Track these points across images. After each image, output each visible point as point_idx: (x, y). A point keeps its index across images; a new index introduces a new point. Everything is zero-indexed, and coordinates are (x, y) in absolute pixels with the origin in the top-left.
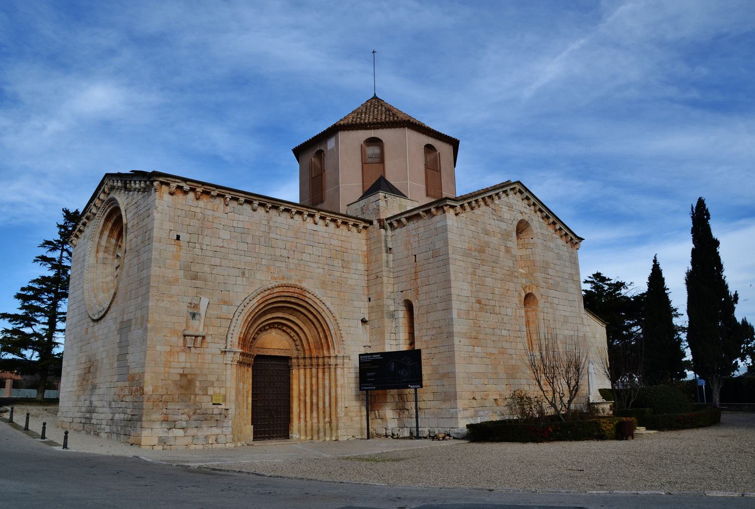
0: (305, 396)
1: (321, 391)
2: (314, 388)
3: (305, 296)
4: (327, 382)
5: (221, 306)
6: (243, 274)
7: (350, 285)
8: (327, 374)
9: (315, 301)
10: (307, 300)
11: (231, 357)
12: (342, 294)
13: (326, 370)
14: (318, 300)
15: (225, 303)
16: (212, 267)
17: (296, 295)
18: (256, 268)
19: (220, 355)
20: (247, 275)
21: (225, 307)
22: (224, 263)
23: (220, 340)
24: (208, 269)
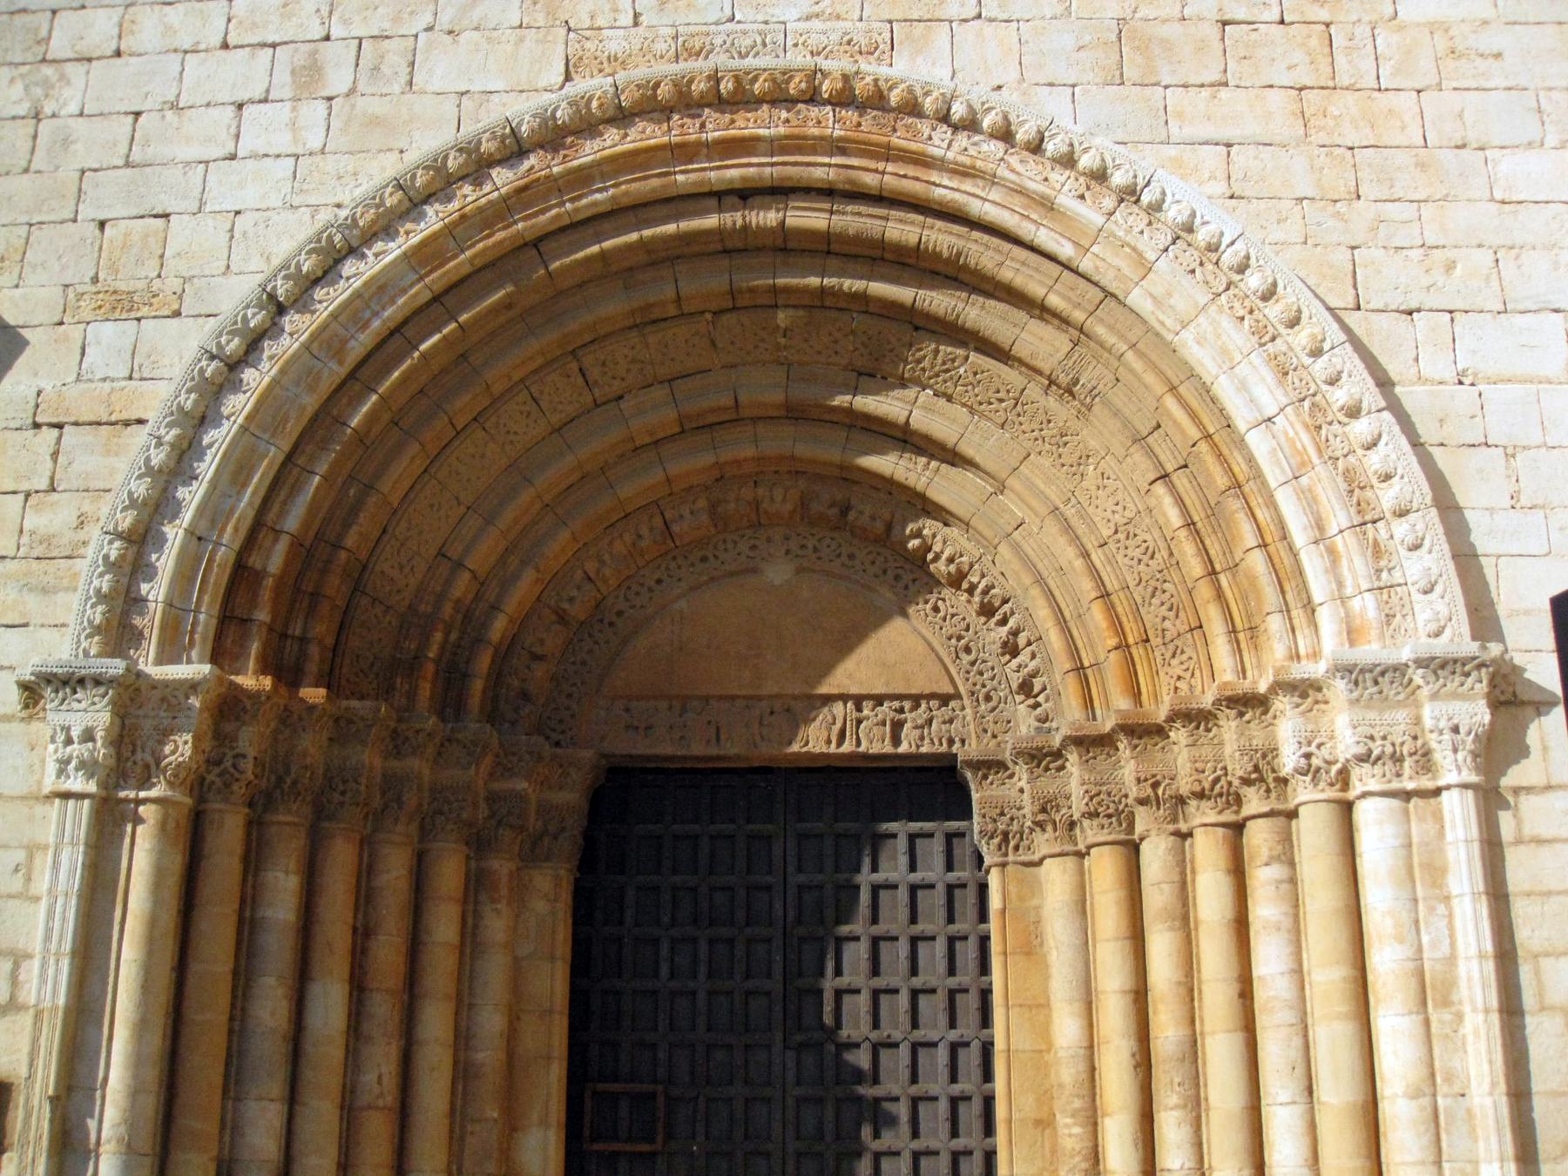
0: (1092, 1120)
1: (1221, 1052)
2: (1167, 1032)
3: (922, 161)
4: (1269, 960)
5: (75, 332)
6: (309, 77)
7: (1433, 27)
8: (1264, 877)
9: (1035, 186)
10: (945, 189)
11: (88, 736)
12: (1344, 103)
13: (1259, 837)
14: (1058, 176)
15: (122, 306)
16: (48, 71)
17: (823, 169)
18: (427, 19)
19: (17, 727)
20: (338, 80)
21: (109, 337)
22: (150, 26)
23: (33, 602)
24: (18, 90)
